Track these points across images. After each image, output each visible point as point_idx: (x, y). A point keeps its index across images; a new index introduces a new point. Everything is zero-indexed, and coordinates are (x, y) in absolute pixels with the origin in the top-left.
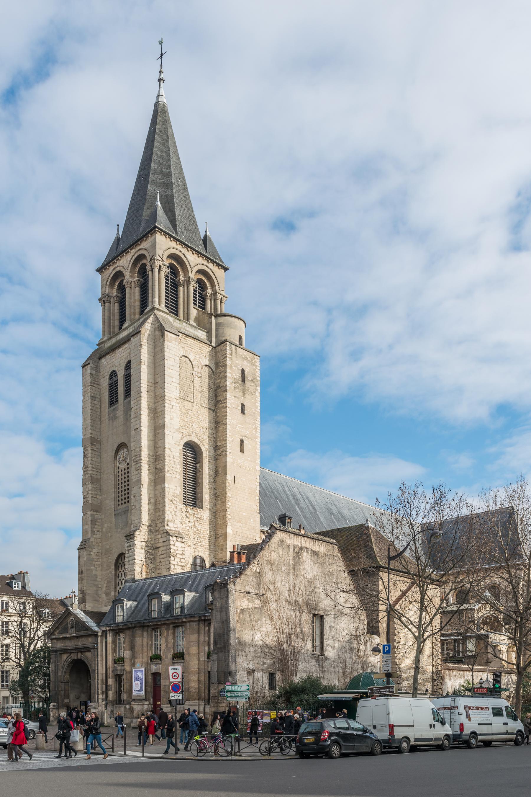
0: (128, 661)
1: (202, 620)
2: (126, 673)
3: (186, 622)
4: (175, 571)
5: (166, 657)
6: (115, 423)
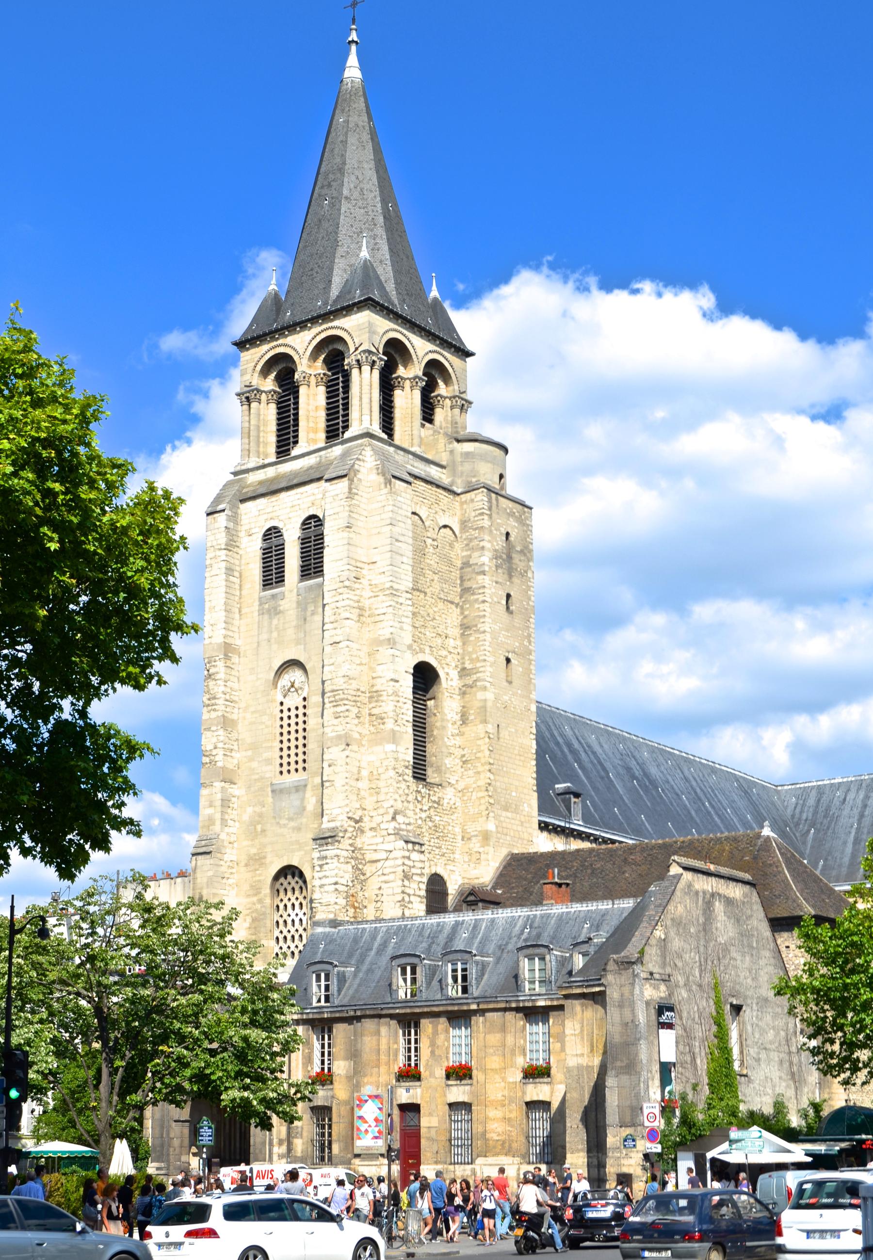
0: (344, 1080)
1: (511, 1009)
3: (475, 1012)
4: (410, 906)
5: (432, 1075)
6: (275, 621)
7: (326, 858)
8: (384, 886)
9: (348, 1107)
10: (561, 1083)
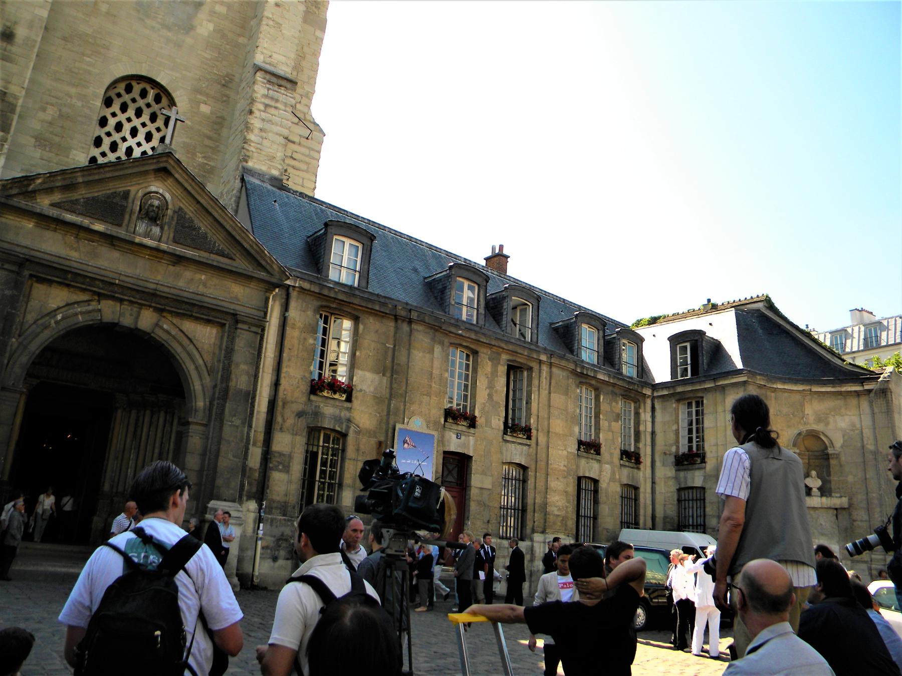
2: (358, 433)
5: (488, 423)
7: (277, 101)
8: (290, 170)
9: (373, 441)
10: (607, 463)
